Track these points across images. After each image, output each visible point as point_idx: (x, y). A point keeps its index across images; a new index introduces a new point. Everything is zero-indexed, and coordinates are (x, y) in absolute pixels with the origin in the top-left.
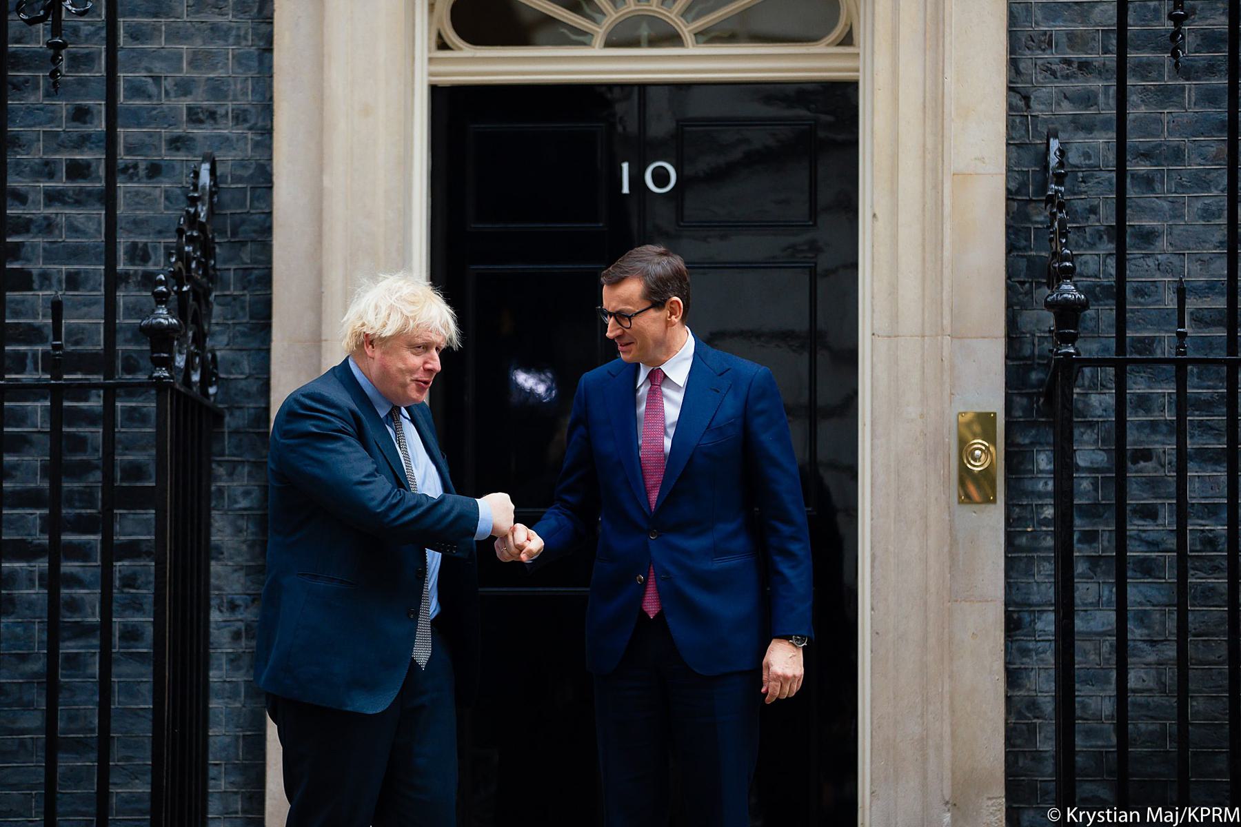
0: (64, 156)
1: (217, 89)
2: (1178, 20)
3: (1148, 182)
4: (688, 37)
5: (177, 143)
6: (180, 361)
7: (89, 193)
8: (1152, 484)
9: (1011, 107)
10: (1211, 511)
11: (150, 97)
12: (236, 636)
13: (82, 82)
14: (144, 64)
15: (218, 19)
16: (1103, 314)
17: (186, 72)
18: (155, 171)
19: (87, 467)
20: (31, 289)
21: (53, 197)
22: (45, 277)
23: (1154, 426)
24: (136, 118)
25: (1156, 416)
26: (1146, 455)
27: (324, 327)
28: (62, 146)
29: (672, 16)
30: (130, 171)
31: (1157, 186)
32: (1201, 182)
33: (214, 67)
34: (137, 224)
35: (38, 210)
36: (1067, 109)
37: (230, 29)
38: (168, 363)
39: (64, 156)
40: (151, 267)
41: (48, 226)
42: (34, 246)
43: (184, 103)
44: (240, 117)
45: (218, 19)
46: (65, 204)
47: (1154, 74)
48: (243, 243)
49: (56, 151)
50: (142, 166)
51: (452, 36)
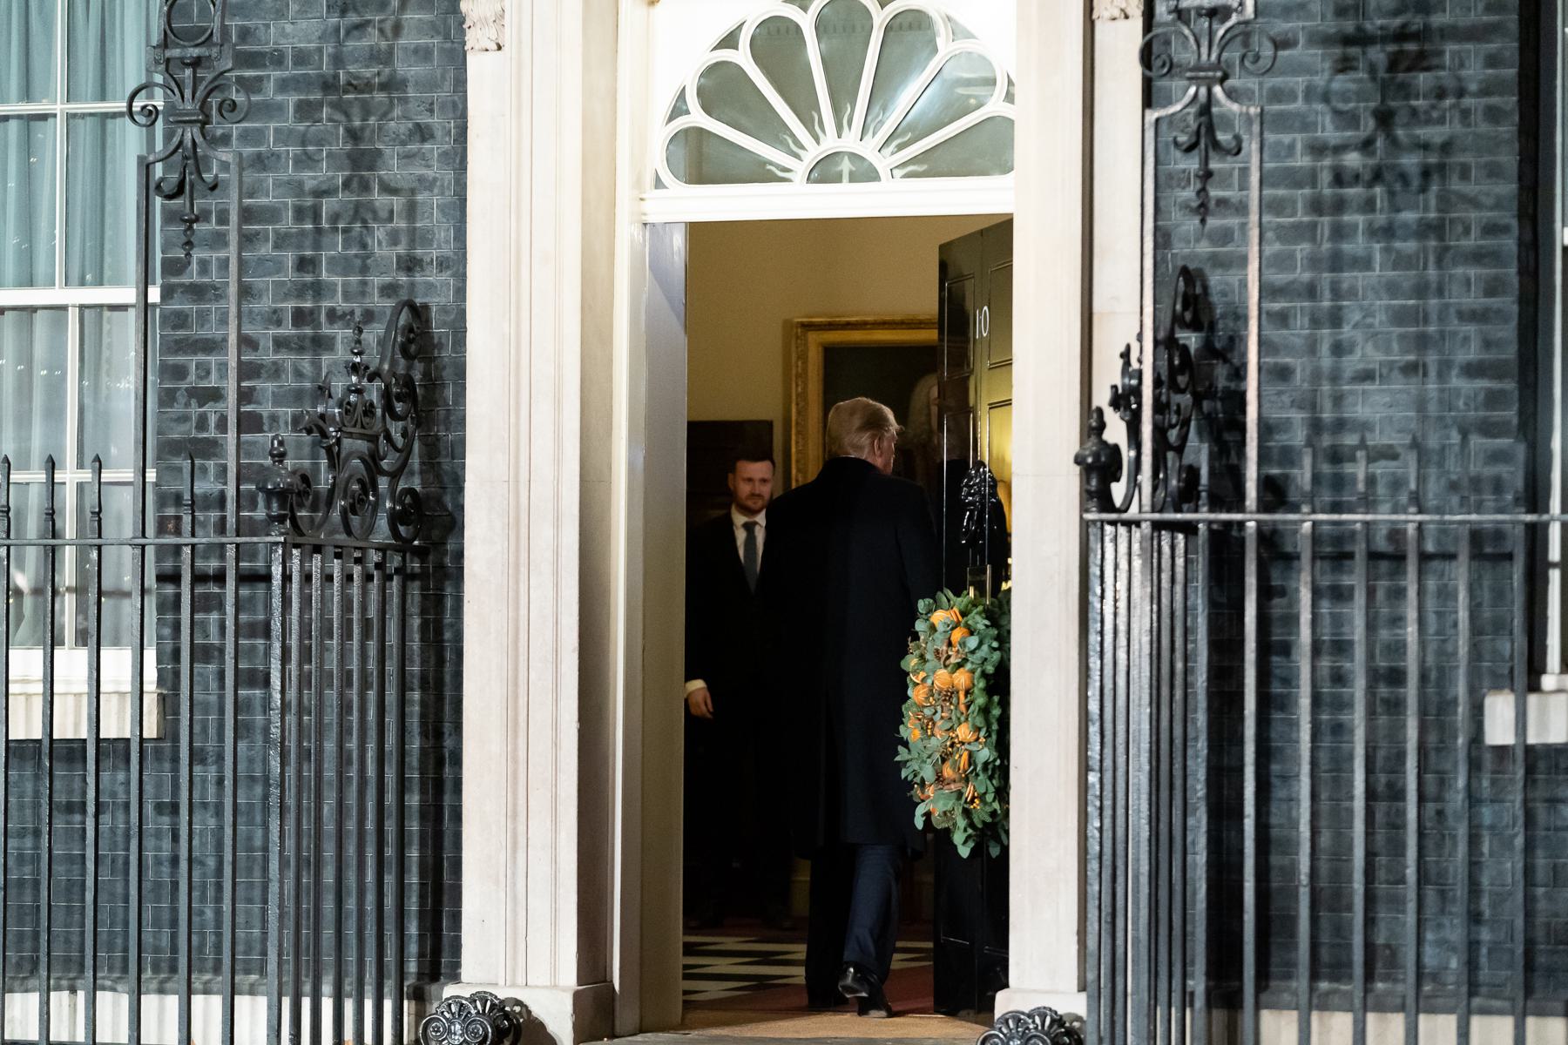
4: (883, 172)
15: (424, 171)
20: (261, 431)
21: (280, 343)
22: (274, 418)
28: (286, 297)
29: (868, 149)
31: (1291, 321)
37: (435, 179)
41: (276, 371)
42: (264, 390)
44: (443, 264)
45: (424, 171)
47: (1288, 211)
49: (283, 301)
50: (358, 313)
51: (667, 176)
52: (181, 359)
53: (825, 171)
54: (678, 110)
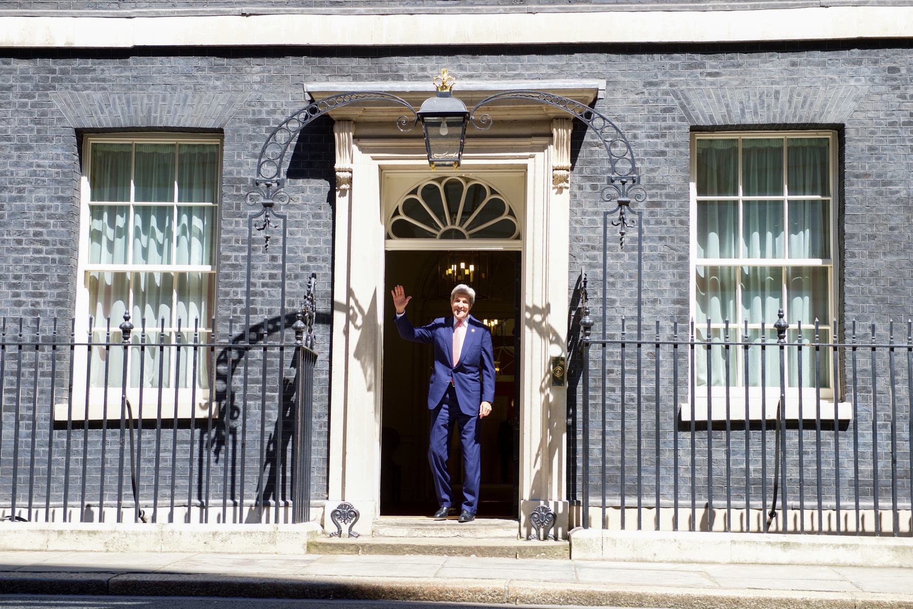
0: (268, 271)
1: (317, 250)
2: (623, 234)
3: (613, 284)
5: (303, 268)
6: (304, 337)
8: (613, 381)
9: (570, 259)
10: (632, 389)
12: (321, 426)
13: (274, 248)
16: (598, 327)
17: (307, 245)
18: (297, 277)
19: (274, 371)
21: (264, 285)
22: (261, 310)
23: (614, 362)
24: (291, 260)
25: (615, 359)
26: (611, 371)
29: (462, 229)
32: (630, 284)
33: (316, 243)
34: (291, 294)
35: (259, 289)
36: (587, 261)
38: (300, 339)
39: (268, 271)
40: (295, 307)
41: (262, 294)
52: (227, 289)
53: (447, 235)
54: (397, 213)
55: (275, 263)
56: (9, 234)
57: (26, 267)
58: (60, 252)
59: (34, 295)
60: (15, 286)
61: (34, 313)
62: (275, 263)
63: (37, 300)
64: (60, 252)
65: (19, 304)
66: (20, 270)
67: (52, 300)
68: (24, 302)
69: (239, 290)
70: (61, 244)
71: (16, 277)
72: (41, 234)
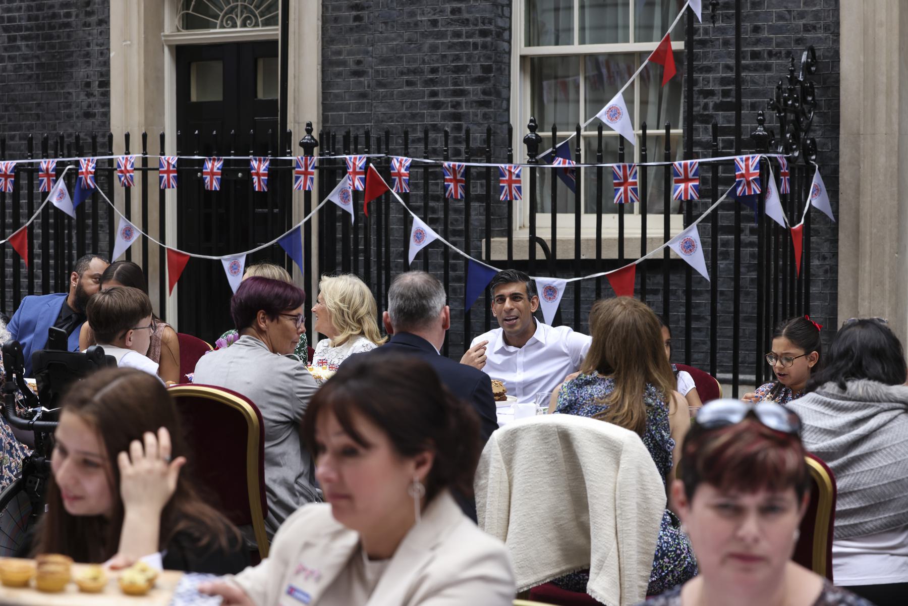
5: (798, 41)
7: (760, 66)
11: (787, 20)
13: (757, 14)
14: (785, 4)
27: (862, 129)
30: (777, 55)
43: (801, 22)
46: (750, 71)
48: (828, 88)
50: (783, 52)
55: (761, 36)
56: (423, 14)
57: (444, 56)
58: (484, 33)
59: (456, 93)
60: (432, 82)
61: (457, 117)
62: (761, 36)
63: (458, 99)
64: (484, 33)
65: (437, 105)
66: (437, 61)
67: (475, 98)
68: (443, 103)
69: (711, 76)
70: (483, 23)
71: (434, 71)
72: (459, 10)
